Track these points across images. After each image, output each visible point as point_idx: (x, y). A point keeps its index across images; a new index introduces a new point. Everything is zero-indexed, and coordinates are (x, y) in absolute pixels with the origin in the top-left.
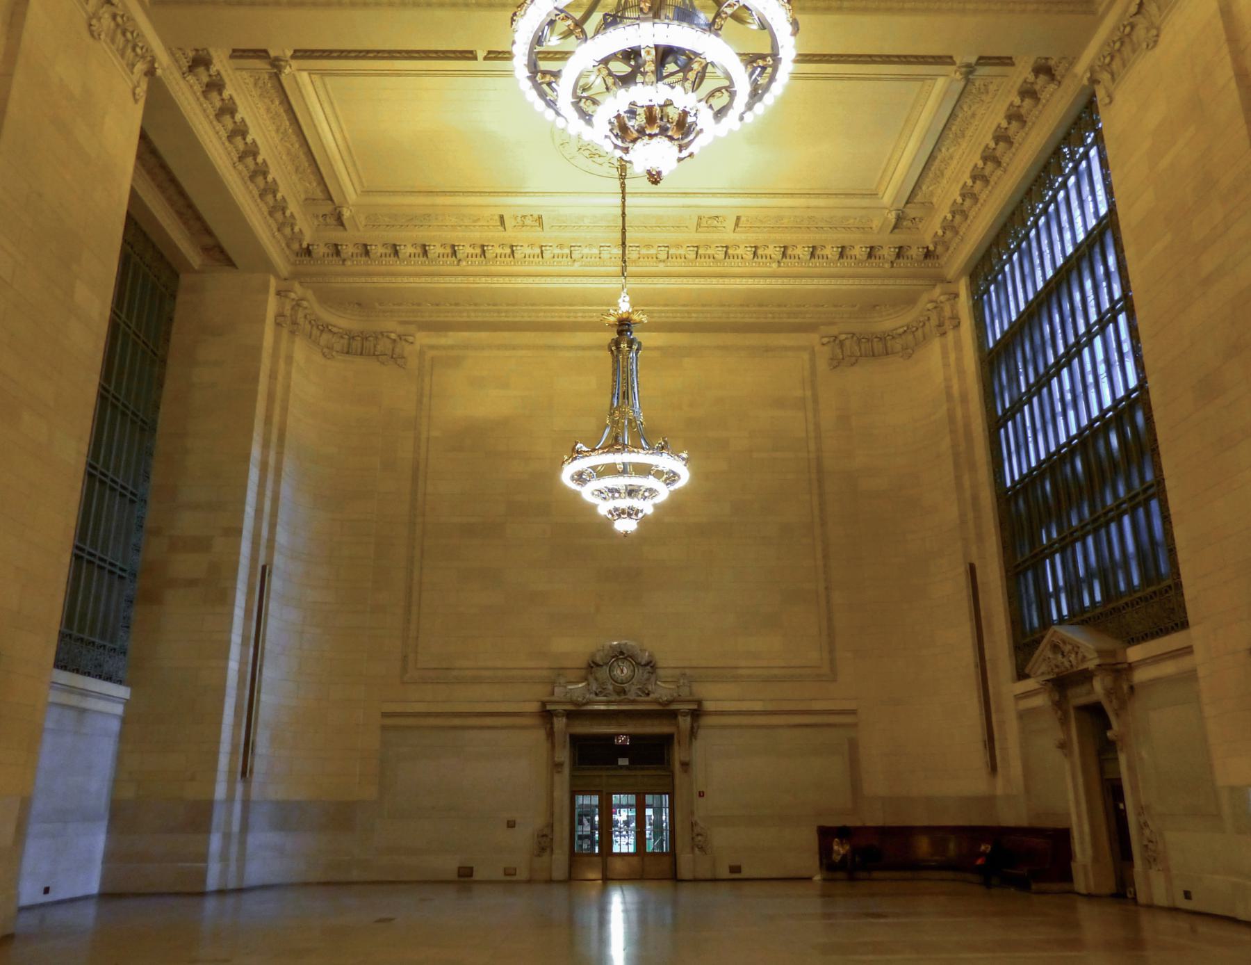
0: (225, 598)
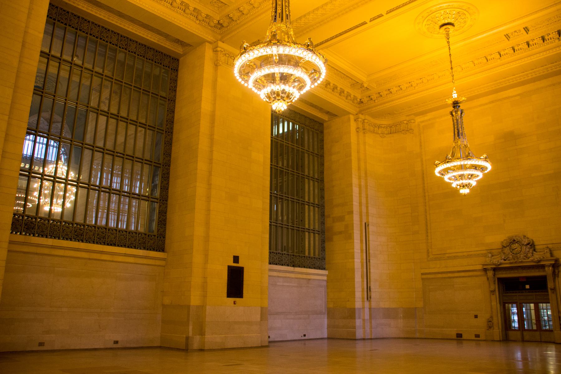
0: (349, 237)
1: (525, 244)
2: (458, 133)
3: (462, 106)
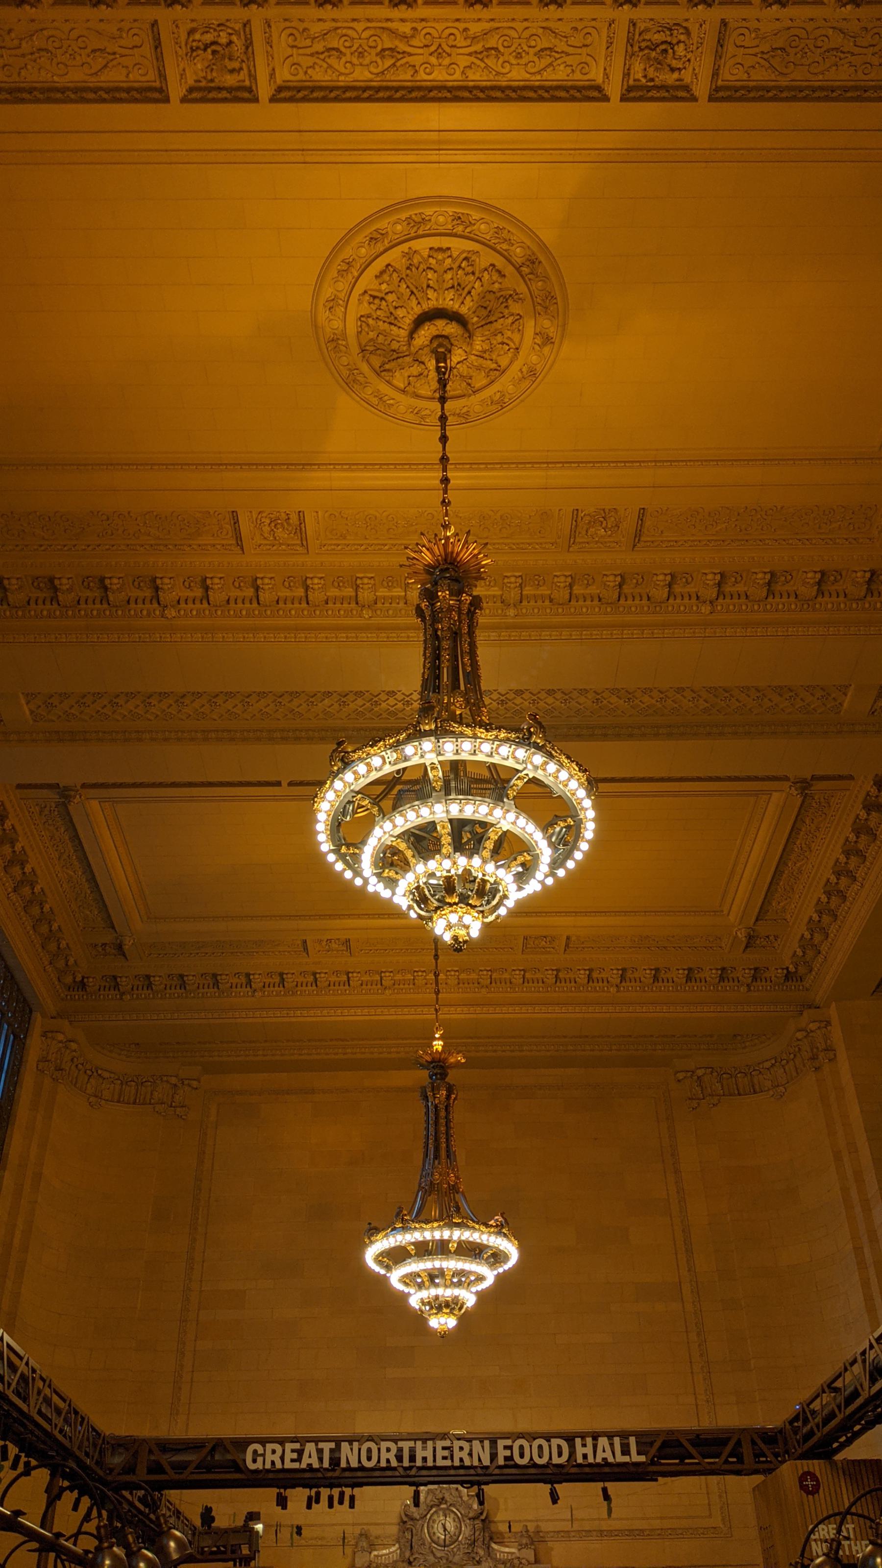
1: (471, 1515)
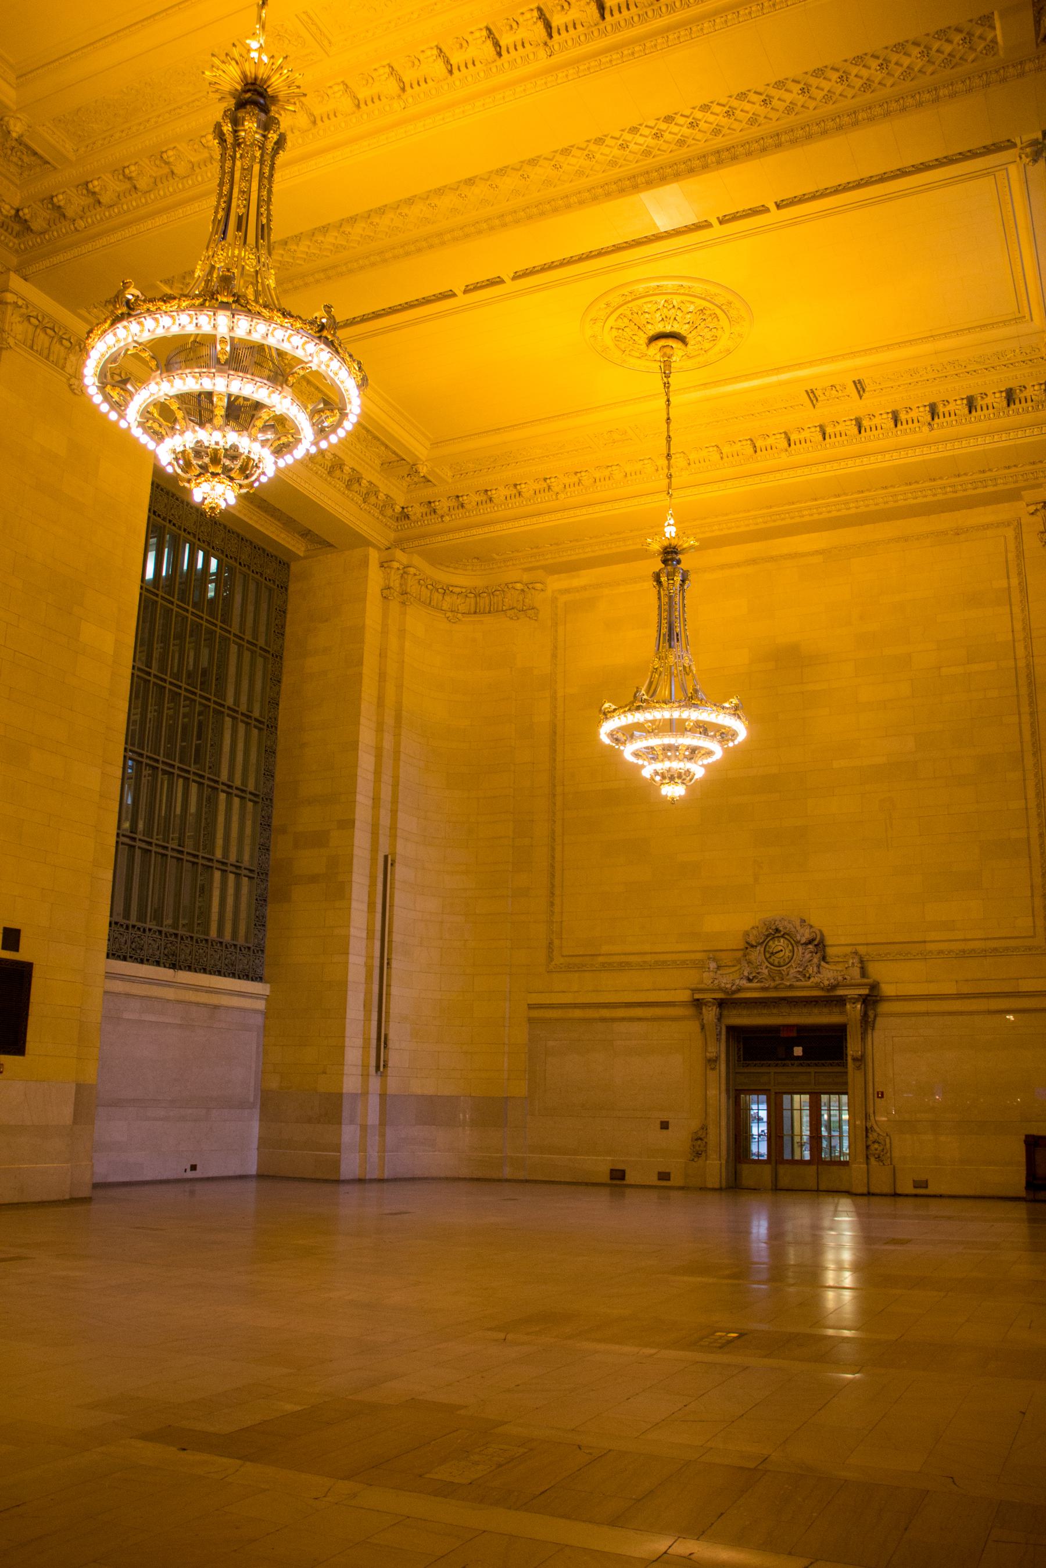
1: (803, 940)
2: (670, 636)
3: (687, 562)
